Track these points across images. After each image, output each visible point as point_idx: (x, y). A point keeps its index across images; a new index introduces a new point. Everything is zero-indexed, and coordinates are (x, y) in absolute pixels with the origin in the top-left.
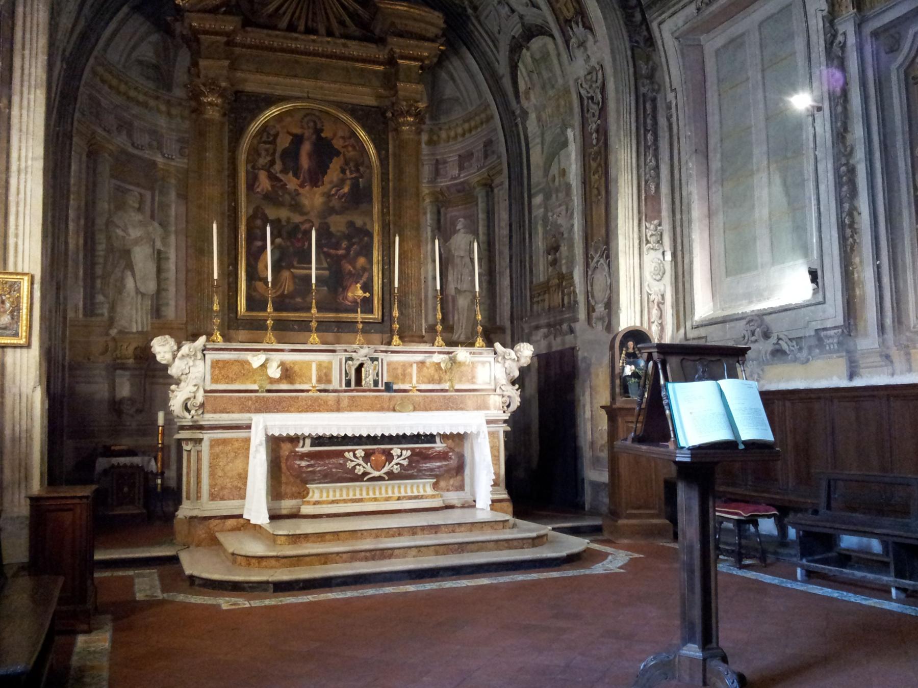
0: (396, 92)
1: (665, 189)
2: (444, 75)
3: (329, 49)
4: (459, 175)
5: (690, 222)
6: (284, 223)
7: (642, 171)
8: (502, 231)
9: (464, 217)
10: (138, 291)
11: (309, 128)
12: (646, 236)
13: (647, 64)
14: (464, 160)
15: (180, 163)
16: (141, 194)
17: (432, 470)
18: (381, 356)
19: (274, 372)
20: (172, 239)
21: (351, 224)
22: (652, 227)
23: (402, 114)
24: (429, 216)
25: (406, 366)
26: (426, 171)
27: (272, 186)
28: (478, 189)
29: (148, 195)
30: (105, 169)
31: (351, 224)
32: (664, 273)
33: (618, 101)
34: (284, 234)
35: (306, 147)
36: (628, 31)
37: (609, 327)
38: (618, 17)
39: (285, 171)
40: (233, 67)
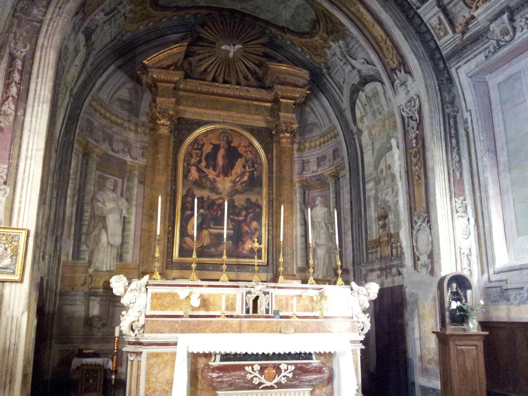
0: (279, 119)
2: (308, 109)
3: (237, 93)
4: (317, 170)
5: (487, 198)
6: (206, 199)
7: (450, 163)
9: (321, 197)
10: (109, 243)
11: (223, 140)
12: (456, 207)
13: (449, 94)
14: (320, 160)
15: (142, 161)
16: (115, 181)
17: (310, 381)
19: (196, 302)
21: (248, 200)
22: (460, 202)
23: (282, 132)
24: (298, 195)
25: (287, 299)
26: (297, 167)
27: (199, 176)
28: (329, 179)
29: (120, 181)
30: (93, 165)
31: (248, 200)
32: (470, 234)
33: (431, 118)
34: (206, 208)
36: (436, 74)
37: (432, 272)
39: (207, 167)
40: (178, 103)
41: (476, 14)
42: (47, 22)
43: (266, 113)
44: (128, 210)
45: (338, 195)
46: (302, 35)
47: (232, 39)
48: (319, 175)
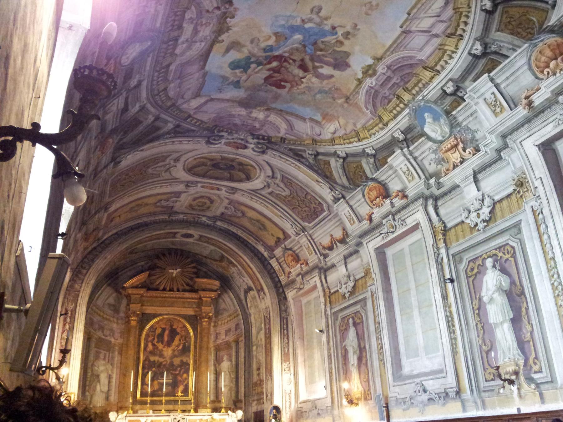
1: (291, 350)
2: (221, 300)
3: (178, 296)
8: (242, 359)
9: (227, 355)
10: (101, 391)
14: (228, 332)
15: (120, 341)
18: (186, 417)
20: (115, 370)
21: (182, 361)
26: (212, 338)
28: (233, 343)
30: (93, 345)
31: (182, 361)
35: (167, 333)
37: (272, 403)
38: (274, 291)
39: (158, 342)
40: (142, 305)
41: (291, 271)
42: (82, 291)
43: (194, 306)
44: (112, 370)
45: (237, 353)
46: (216, 260)
47: (174, 265)
48: (227, 341)
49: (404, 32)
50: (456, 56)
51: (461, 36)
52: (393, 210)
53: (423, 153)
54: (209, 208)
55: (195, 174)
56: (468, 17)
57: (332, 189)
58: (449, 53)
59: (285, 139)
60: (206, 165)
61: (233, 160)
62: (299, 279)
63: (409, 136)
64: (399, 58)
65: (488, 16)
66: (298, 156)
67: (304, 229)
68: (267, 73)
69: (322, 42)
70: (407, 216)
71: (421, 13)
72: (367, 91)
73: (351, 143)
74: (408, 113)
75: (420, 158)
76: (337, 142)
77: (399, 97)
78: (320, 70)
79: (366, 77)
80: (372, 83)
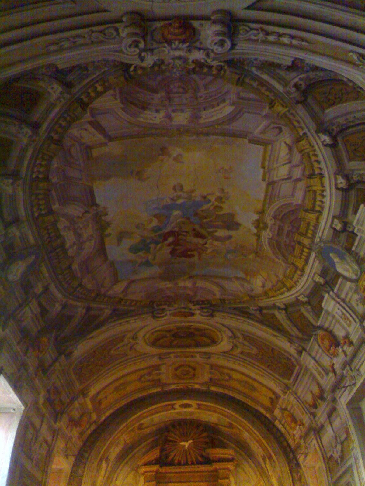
13: (297, 475)
49: (268, 184)
50: (327, 193)
51: (321, 174)
52: (348, 358)
53: (347, 294)
54: (194, 375)
55: (162, 346)
56: (316, 155)
57: (291, 341)
58: (319, 192)
59: (224, 300)
60: (166, 337)
61: (189, 327)
62: (302, 441)
63: (328, 278)
64: (280, 207)
65: (333, 149)
66: (244, 313)
67: (288, 388)
68: (169, 249)
69: (202, 211)
70: (359, 365)
71: (273, 164)
72: (269, 243)
73: (282, 294)
74: (316, 257)
75: (347, 300)
76: (270, 294)
77: (299, 243)
78: (217, 234)
79: (260, 231)
80: (268, 235)
